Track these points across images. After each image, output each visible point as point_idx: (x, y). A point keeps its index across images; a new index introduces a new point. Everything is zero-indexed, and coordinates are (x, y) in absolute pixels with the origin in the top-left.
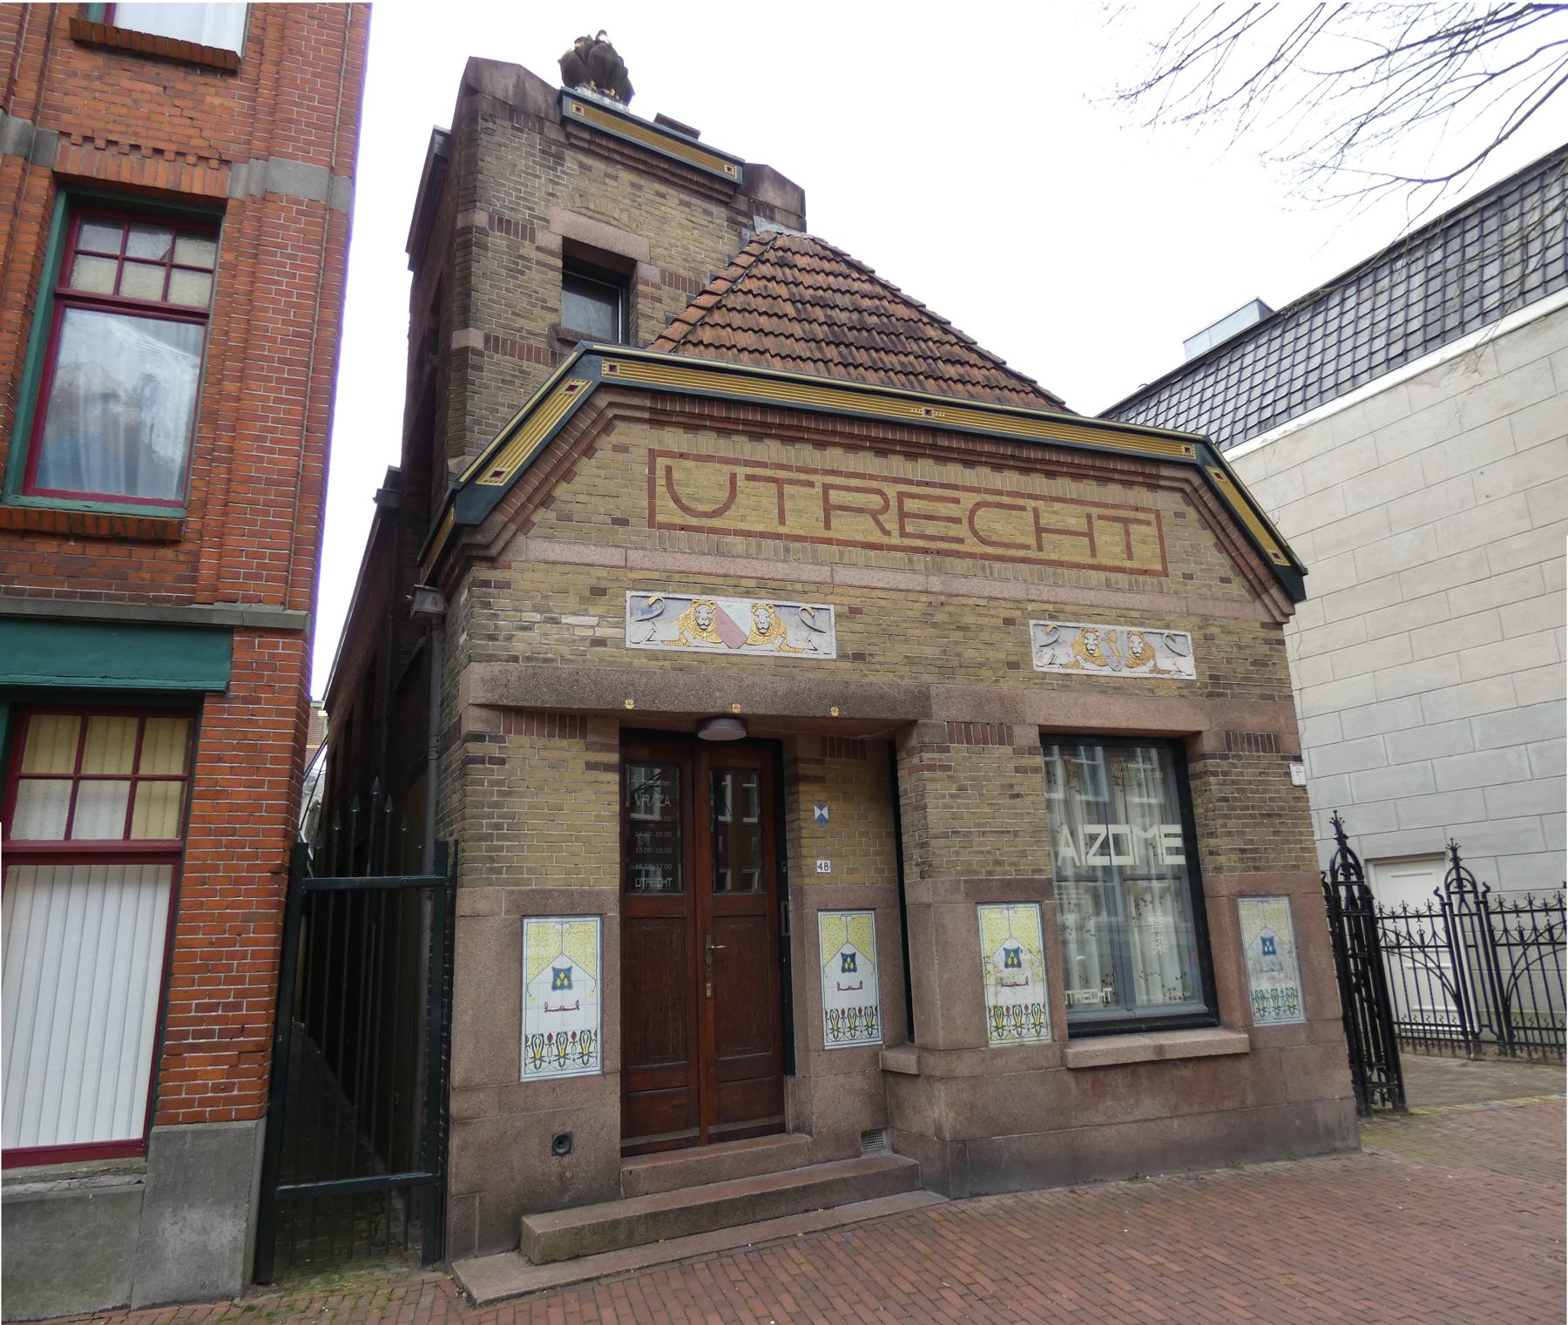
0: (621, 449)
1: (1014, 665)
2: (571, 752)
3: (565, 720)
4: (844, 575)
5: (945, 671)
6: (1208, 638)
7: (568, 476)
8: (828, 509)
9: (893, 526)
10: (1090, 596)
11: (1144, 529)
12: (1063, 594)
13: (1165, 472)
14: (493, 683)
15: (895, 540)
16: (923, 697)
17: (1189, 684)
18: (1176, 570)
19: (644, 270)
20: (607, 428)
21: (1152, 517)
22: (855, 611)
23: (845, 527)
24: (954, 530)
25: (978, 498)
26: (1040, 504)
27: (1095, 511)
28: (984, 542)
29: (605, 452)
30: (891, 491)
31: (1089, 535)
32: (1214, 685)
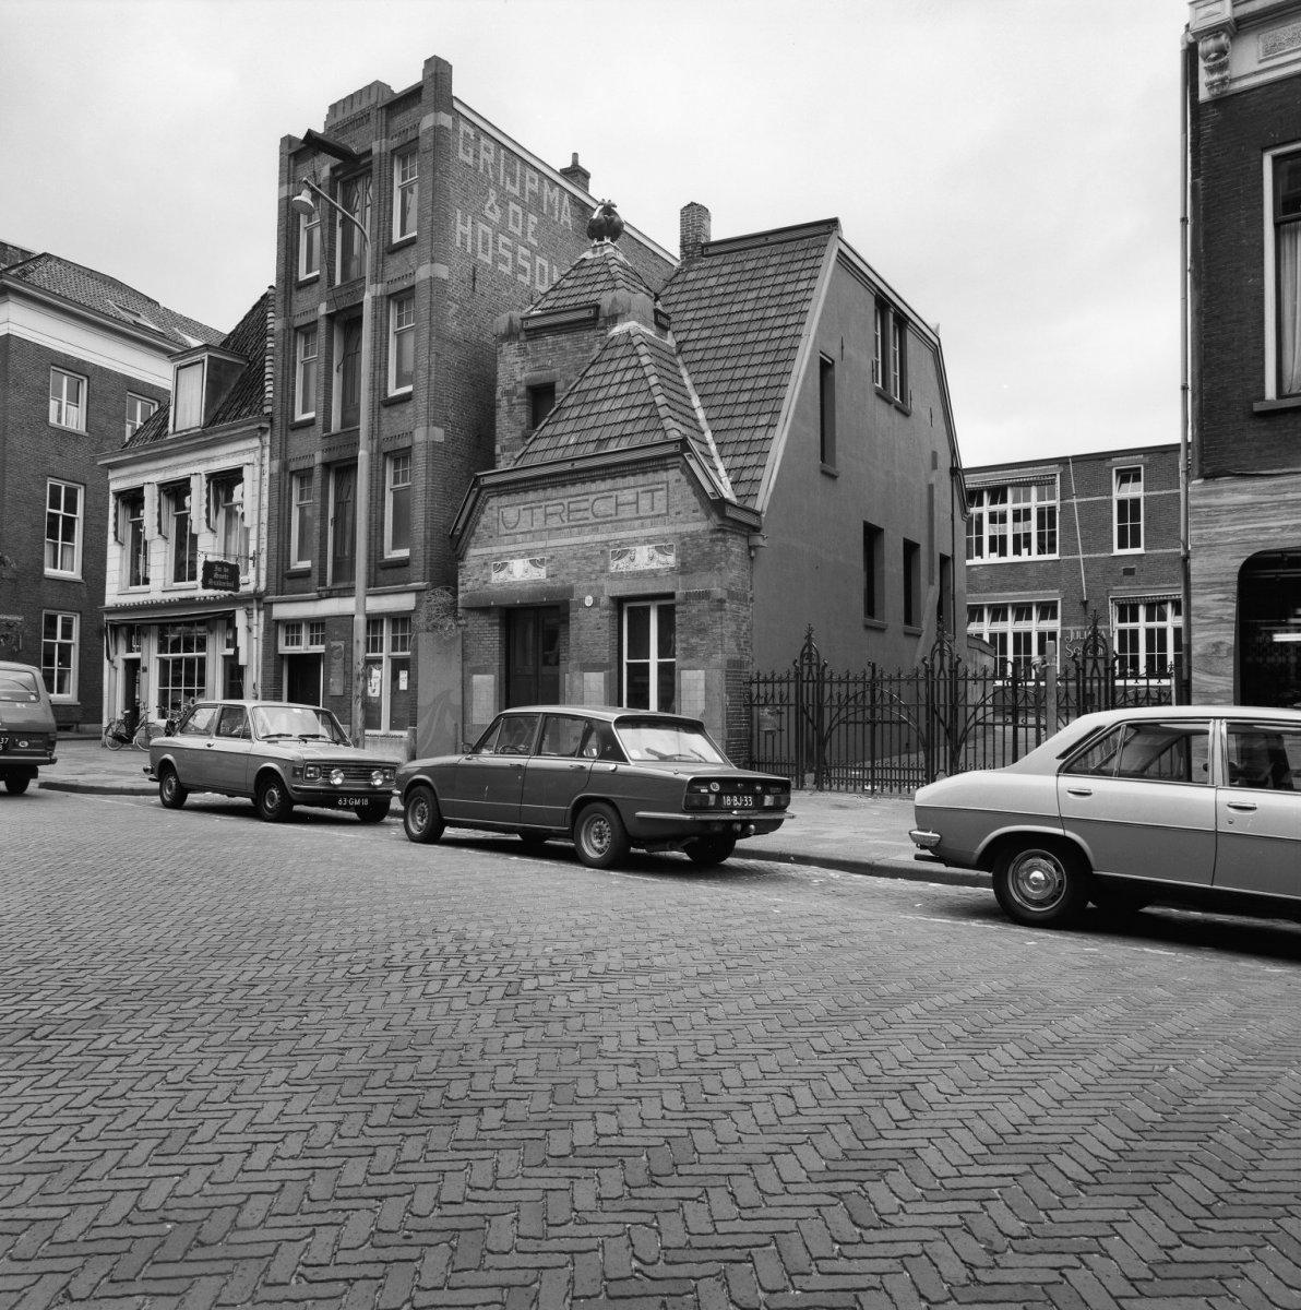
0: (491, 509)
1: (603, 572)
2: (483, 621)
3: (485, 610)
4: (552, 543)
5: (579, 578)
6: (684, 544)
7: (477, 524)
8: (546, 515)
9: (565, 518)
10: (634, 533)
11: (661, 493)
12: (623, 535)
13: (669, 461)
14: (463, 600)
15: (566, 524)
16: (570, 590)
17: (672, 569)
18: (672, 512)
19: (559, 386)
20: (487, 502)
21: (664, 486)
22: (552, 557)
23: (554, 522)
24: (586, 514)
25: (594, 497)
26: (619, 493)
27: (640, 490)
28: (597, 517)
29: (487, 511)
30: (565, 502)
31: (637, 502)
32: (684, 569)
